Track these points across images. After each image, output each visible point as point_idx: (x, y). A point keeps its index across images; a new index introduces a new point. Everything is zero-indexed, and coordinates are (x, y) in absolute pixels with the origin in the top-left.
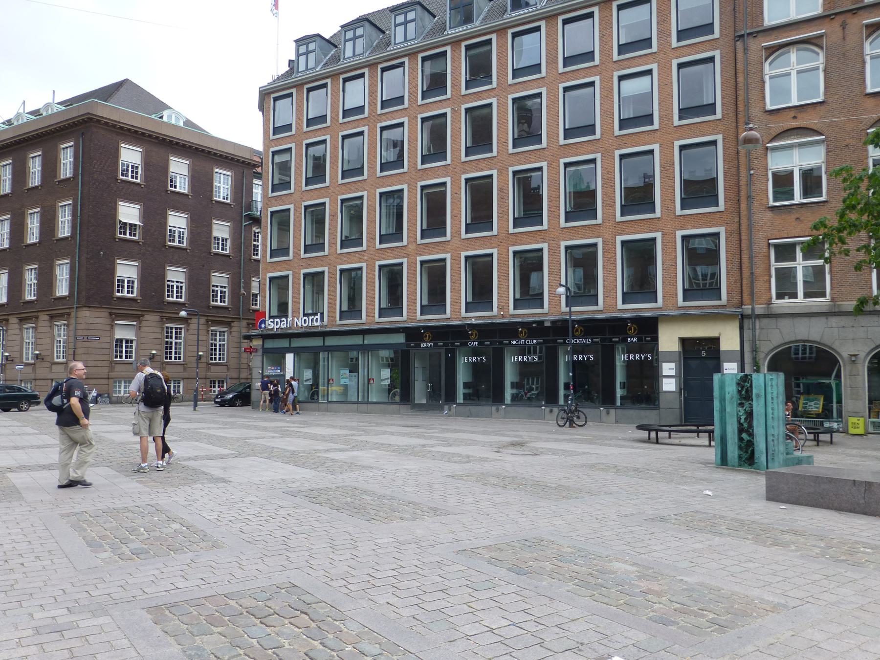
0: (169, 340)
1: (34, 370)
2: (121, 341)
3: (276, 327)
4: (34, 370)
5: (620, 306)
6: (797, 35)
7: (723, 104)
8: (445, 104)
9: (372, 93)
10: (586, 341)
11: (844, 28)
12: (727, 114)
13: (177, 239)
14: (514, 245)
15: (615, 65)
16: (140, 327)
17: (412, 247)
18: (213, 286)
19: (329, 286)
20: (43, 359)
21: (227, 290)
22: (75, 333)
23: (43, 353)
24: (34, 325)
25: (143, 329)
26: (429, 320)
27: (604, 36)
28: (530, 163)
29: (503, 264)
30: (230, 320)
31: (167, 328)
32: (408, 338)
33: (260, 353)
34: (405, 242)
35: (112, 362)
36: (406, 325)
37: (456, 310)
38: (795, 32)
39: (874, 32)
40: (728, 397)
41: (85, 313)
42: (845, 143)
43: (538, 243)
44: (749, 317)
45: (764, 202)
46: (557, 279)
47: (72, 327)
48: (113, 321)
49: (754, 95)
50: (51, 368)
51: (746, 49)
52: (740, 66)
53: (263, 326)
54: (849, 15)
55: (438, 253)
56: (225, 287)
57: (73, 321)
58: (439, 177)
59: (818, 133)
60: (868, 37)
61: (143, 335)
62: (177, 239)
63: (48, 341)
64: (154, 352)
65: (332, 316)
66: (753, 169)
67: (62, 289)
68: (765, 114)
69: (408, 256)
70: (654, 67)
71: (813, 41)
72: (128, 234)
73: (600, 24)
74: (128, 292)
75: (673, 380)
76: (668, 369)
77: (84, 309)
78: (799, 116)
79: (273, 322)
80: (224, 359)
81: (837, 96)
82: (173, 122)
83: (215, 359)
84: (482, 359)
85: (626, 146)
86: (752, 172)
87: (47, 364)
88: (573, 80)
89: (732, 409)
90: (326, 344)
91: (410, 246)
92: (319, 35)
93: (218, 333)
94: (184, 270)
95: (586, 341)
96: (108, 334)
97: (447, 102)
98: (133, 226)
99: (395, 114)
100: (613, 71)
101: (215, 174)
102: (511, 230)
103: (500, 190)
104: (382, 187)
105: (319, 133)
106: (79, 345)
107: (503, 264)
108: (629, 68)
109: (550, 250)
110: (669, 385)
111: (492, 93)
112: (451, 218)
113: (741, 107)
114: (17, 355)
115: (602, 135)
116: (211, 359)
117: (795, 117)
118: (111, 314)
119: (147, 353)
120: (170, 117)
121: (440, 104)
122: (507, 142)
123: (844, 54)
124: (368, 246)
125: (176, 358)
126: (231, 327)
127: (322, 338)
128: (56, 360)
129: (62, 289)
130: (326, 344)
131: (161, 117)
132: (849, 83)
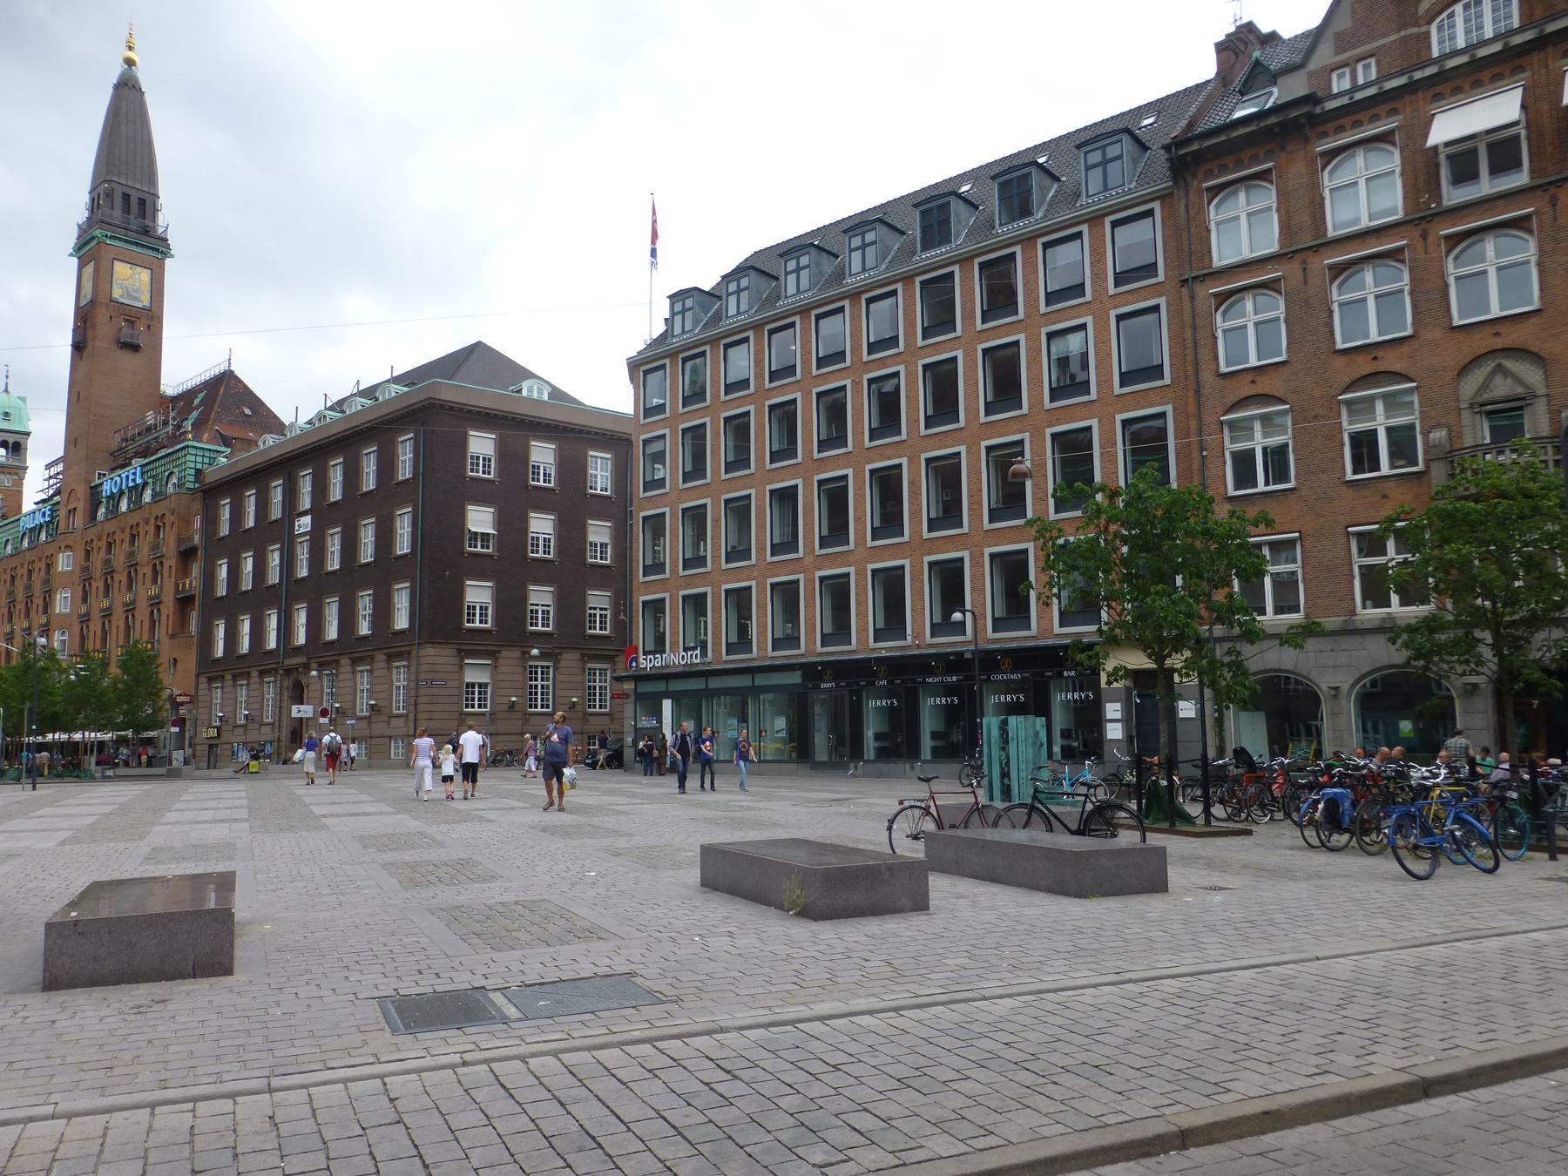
0: (533, 683)
1: (369, 724)
2: (473, 685)
3: (649, 666)
4: (369, 724)
5: (1057, 629)
6: (1252, 278)
7: (1171, 365)
9: (759, 363)
10: (1014, 677)
12: (1178, 378)
13: (541, 548)
15: (1043, 320)
16: (496, 667)
17: (809, 559)
18: (590, 608)
19: (712, 611)
20: (379, 711)
21: (608, 613)
22: (417, 675)
23: (381, 703)
24: (368, 667)
25: (499, 670)
26: (832, 654)
28: (946, 447)
29: (916, 578)
30: (613, 653)
31: (531, 666)
32: (805, 677)
33: (632, 699)
35: (462, 713)
36: (804, 660)
37: (862, 640)
38: (1248, 275)
39: (1341, 273)
40: (993, 741)
41: (429, 651)
42: (1314, 413)
43: (957, 550)
44: (1207, 640)
45: (1221, 490)
46: (982, 596)
47: (413, 669)
48: (462, 659)
49: (1204, 354)
50: (389, 722)
51: (1193, 298)
53: (634, 664)
54: (1309, 253)
56: (606, 609)
57: (414, 661)
59: (1283, 401)
60: (1332, 281)
61: (501, 677)
62: (541, 548)
63: (385, 687)
64: (514, 699)
65: (716, 651)
66: (1206, 449)
67: (402, 622)
68: (1218, 379)
69: (804, 571)
70: (1089, 320)
71: (1272, 286)
72: (479, 546)
73: (1024, 267)
74: (481, 622)
75: (1119, 725)
76: (1113, 710)
77: (428, 645)
78: (1259, 380)
79: (645, 659)
80: (606, 706)
81: (1301, 355)
82: (535, 396)
83: (595, 707)
84: (1018, 698)
85: (1059, 422)
86: (1205, 453)
87: (385, 718)
89: (995, 752)
90: (756, 684)
91: (807, 559)
92: (696, 289)
93: (598, 672)
94: (551, 589)
95: (1014, 677)
96: (457, 676)
97: (847, 371)
98: (485, 537)
100: (1040, 327)
101: (589, 459)
102: (926, 535)
103: (911, 483)
104: (772, 483)
106: (422, 692)
107: (916, 578)
108: (1060, 322)
109: (972, 559)
110: (1114, 732)
112: (855, 520)
114: (348, 705)
115: (1030, 408)
116: (590, 707)
117: (1253, 382)
118: (459, 651)
119: (505, 700)
120: (530, 389)
121: (838, 374)
122: (917, 421)
123: (1306, 302)
124: (757, 560)
125: (542, 707)
126: (614, 663)
127: (750, 676)
128: (395, 712)
129: (402, 622)
130: (756, 684)
131: (519, 391)
132: (1314, 337)
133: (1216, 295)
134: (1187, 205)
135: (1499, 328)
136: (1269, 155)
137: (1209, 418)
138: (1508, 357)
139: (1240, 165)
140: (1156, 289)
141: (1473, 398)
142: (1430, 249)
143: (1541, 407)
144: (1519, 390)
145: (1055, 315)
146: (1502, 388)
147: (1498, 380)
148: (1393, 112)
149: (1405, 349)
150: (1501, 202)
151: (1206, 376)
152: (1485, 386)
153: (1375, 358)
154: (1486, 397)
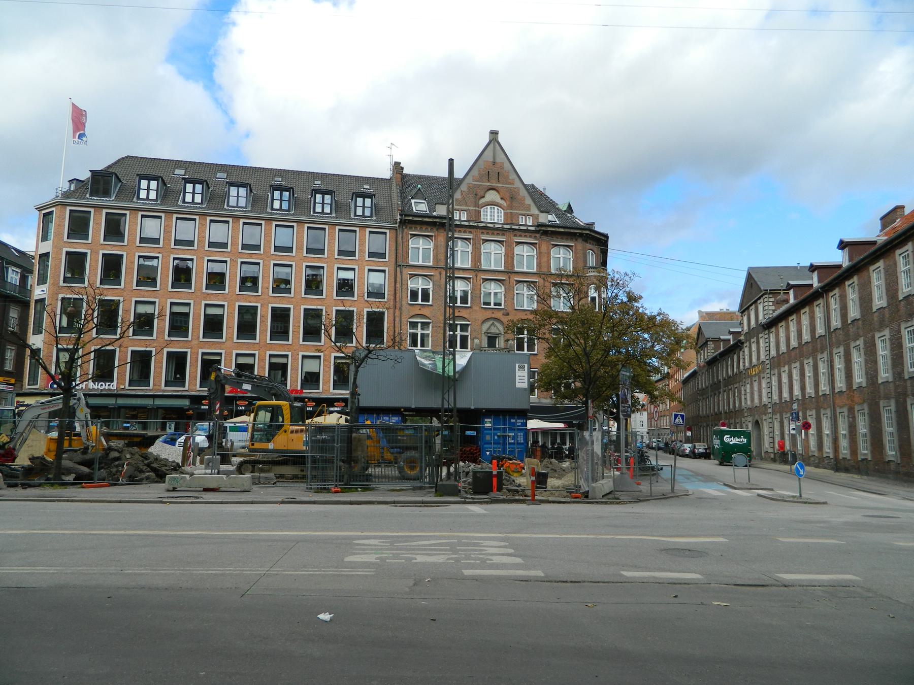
5: (332, 390)
8: (226, 254)
9: (167, 232)
11: (440, 275)
14: (269, 350)
15: (336, 261)
17: (195, 342)
27: (330, 243)
28: (283, 304)
32: (191, 403)
34: (190, 338)
38: (421, 270)
51: (401, 272)
52: (398, 279)
55: (215, 349)
58: (218, 300)
69: (191, 348)
78: (422, 309)
88: (312, 262)
91: (193, 341)
99: (186, 251)
105: (115, 248)
108: (343, 264)
111: (261, 256)
113: (398, 299)
117: (420, 309)
122: (268, 288)
133: (410, 274)
134: (402, 237)
135: (493, 311)
136: (431, 231)
137: (404, 320)
138: (497, 322)
139: (421, 230)
140: (385, 264)
141: (487, 330)
142: (478, 281)
143: (502, 338)
144: (498, 332)
145: (341, 261)
146: (493, 330)
147: (492, 327)
148: (470, 232)
149: (468, 311)
150: (497, 273)
151: (404, 303)
152: (489, 329)
153: (459, 311)
154: (489, 331)
